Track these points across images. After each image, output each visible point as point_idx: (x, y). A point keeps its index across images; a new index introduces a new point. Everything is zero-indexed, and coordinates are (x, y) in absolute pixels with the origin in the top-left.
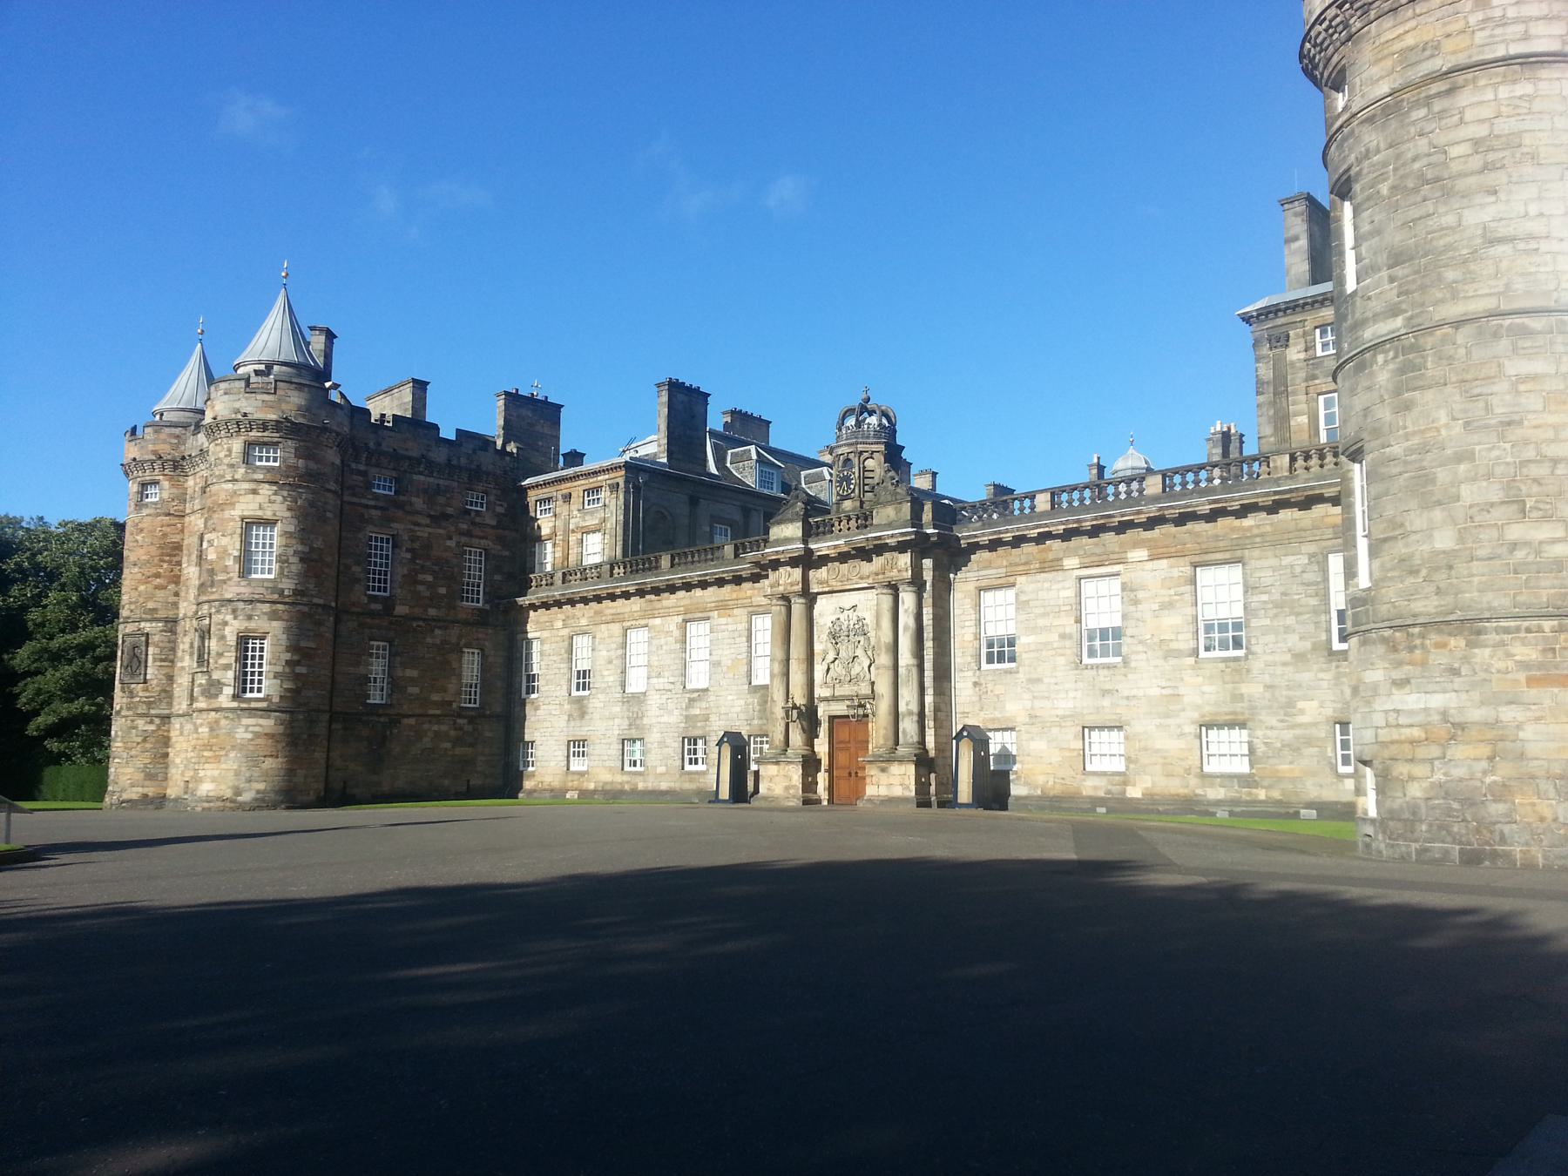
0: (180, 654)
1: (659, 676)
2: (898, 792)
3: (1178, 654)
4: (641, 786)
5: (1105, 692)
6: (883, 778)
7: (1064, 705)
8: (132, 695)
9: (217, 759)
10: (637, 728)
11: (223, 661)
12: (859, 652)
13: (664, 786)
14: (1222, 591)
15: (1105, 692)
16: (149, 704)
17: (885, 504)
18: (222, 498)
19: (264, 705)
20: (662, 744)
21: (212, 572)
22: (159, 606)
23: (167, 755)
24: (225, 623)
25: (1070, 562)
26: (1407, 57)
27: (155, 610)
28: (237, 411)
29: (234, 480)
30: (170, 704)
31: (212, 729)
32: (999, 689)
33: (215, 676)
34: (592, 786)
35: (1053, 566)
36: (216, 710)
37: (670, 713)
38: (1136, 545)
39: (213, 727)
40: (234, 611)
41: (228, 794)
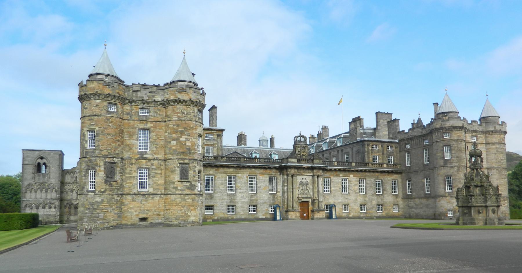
0: (128, 171)
1: (241, 189)
2: (321, 217)
3: (357, 193)
4: (235, 217)
5: (346, 199)
6: (318, 214)
7: (340, 201)
8: (111, 185)
9: (195, 209)
10: (233, 202)
11: (195, 179)
12: (308, 188)
13: (243, 217)
15: (346, 199)
16: (118, 190)
17: (317, 159)
18: (192, 126)
19: (202, 193)
20: (242, 207)
22: (119, 152)
23: (122, 209)
24: (195, 167)
25: (341, 175)
26: (459, 136)
27: (118, 154)
28: (198, 99)
29: (196, 121)
30: (123, 191)
31: (193, 200)
32: (328, 197)
33: (193, 183)
34: (216, 218)
35: (338, 176)
36: (194, 194)
37: (245, 199)
39: (193, 200)
40: (198, 163)
41: (198, 221)
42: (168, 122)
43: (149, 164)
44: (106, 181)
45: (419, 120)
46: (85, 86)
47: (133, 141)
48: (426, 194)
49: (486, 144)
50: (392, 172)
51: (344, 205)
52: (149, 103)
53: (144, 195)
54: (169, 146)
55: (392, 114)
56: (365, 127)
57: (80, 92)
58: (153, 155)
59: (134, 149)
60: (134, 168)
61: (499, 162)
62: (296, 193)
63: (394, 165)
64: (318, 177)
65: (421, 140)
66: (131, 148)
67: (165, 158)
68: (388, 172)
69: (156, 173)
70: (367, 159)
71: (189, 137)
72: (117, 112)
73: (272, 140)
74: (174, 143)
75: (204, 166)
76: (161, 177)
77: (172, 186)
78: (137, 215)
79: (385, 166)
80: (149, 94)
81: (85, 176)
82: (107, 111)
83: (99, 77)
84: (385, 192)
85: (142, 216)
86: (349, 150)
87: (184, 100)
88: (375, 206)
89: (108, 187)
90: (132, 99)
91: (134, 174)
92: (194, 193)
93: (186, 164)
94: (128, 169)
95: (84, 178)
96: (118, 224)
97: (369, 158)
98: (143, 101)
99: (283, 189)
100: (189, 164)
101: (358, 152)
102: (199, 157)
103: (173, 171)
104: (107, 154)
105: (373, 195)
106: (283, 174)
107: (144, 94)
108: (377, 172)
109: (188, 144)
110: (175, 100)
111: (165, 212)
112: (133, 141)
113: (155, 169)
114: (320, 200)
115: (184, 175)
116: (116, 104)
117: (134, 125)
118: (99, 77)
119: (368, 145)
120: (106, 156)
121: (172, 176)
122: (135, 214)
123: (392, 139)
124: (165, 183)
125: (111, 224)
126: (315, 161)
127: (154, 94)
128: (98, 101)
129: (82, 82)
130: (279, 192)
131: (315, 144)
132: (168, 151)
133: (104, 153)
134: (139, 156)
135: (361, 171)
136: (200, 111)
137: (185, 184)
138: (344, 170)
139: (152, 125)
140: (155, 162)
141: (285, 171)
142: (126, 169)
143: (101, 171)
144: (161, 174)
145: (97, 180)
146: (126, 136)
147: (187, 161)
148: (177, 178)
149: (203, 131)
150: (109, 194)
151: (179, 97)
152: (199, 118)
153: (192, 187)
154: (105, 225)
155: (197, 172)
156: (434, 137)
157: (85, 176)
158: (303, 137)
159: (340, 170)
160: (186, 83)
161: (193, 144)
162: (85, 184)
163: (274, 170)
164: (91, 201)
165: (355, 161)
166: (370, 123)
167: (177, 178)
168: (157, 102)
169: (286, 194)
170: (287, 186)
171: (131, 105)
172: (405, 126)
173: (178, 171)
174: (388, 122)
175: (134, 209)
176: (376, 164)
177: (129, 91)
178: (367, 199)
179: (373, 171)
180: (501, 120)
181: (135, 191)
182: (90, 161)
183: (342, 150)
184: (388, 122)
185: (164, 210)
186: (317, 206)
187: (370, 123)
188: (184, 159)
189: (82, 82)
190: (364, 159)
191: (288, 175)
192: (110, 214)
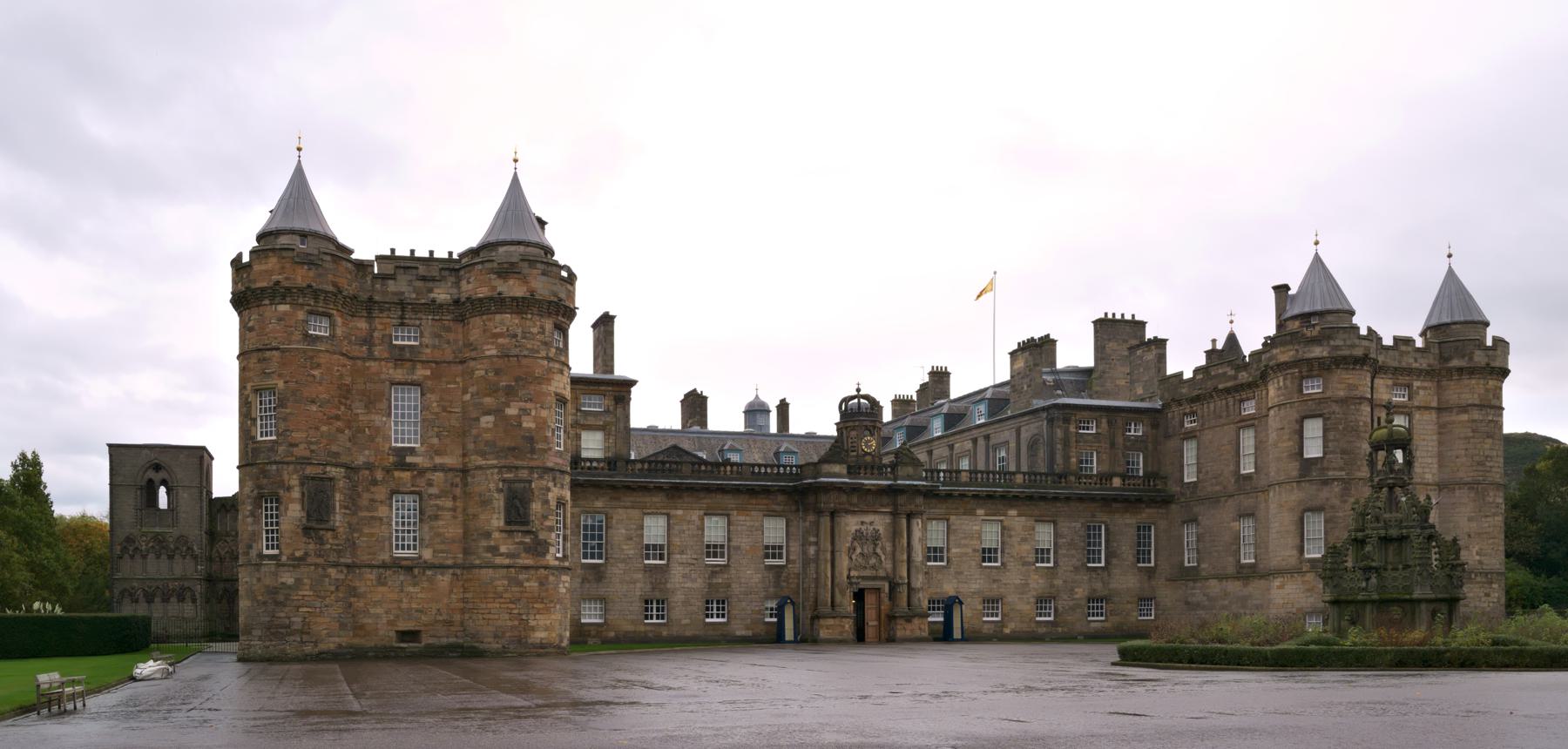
0: (364, 502)
3: (1029, 564)
8: (321, 541)
9: (547, 610)
11: (548, 523)
12: (878, 551)
14: (1044, 535)
17: (906, 464)
18: (538, 372)
21: (531, 440)
24: (548, 490)
25: (980, 512)
27: (337, 454)
30: (354, 555)
31: (541, 584)
33: (542, 536)
35: (972, 513)
36: (546, 568)
38: (1012, 507)
40: (554, 479)
42: (472, 364)
43: (422, 482)
44: (307, 530)
45: (1232, 340)
46: (249, 265)
47: (378, 420)
48: (1243, 566)
49: (1439, 410)
50: (1139, 500)
51: (986, 601)
52: (418, 308)
53: (409, 569)
54: (474, 432)
55: (1142, 324)
56: (1060, 365)
57: (235, 282)
58: (432, 458)
59: (379, 440)
60: (381, 492)
61: (1480, 463)
62: (844, 563)
63: (1147, 476)
64: (909, 516)
65: (1231, 401)
66: (372, 439)
67: (465, 464)
68: (1126, 500)
69: (439, 508)
70: (1059, 459)
71: (529, 405)
72: (333, 336)
73: (783, 407)
74: (487, 421)
75: (575, 486)
76: (455, 517)
77: (484, 543)
78: (390, 623)
79: (1117, 482)
80: (419, 284)
81: (253, 514)
82: (306, 336)
83: (284, 240)
84: (1114, 561)
85: (404, 626)
86: (1006, 434)
87: (514, 299)
88: (1084, 602)
89: (311, 546)
90: (370, 299)
91: (382, 511)
92: (543, 563)
93: (520, 481)
94: (366, 495)
95: (250, 520)
96: (340, 646)
97: (1067, 458)
98: (402, 304)
99: (805, 553)
100: (530, 482)
101: (1033, 445)
102: (559, 461)
103: (485, 503)
104: (307, 454)
105: (1076, 569)
106: (806, 511)
107: (402, 286)
108: (1092, 499)
109: (528, 424)
110: (491, 298)
111: (467, 616)
112: (378, 420)
113: (438, 497)
114: (918, 581)
115: (517, 514)
116: (329, 316)
117: (378, 374)
118: (284, 240)
119: (1067, 421)
120: (304, 462)
121: (482, 517)
122: (384, 620)
123: (1142, 400)
124: (466, 534)
125: (322, 647)
126: (901, 471)
127: (430, 284)
128: (283, 308)
129: (240, 255)
130: (794, 562)
131: (907, 422)
132: (471, 446)
133: (301, 451)
134: (391, 459)
135: (1043, 498)
136: (563, 330)
137: (518, 538)
138: (990, 497)
139: (428, 373)
140: (438, 476)
141: (811, 499)
142: (359, 496)
143: (292, 501)
144: (454, 509)
145: (283, 527)
146: (357, 404)
147: (524, 474)
148: (498, 521)
149: (568, 388)
150: (316, 565)
151: (499, 289)
152: (558, 348)
153: (539, 548)
154: (308, 649)
155: (553, 504)
156: (1272, 392)
157: (253, 514)
158: (866, 397)
159: (976, 496)
160: (522, 249)
161: (542, 424)
162: (255, 536)
163: (780, 498)
164: (268, 581)
165: (1024, 468)
166: (1076, 352)
167: (496, 521)
168: (441, 306)
169: (813, 566)
170: (816, 543)
171: (370, 318)
172: (1183, 361)
173: (499, 501)
174: (1132, 349)
175: (386, 608)
176: (1091, 477)
177: (364, 276)
178: (1059, 582)
179: (1081, 499)
180: (1490, 333)
181: (385, 557)
182: (264, 473)
183: (987, 437)
184: (1132, 349)
185: (463, 611)
186: (905, 604)
187: (1076, 352)
188: (517, 468)
189: (240, 255)
190: (1052, 461)
191: (819, 512)
192: (319, 620)
